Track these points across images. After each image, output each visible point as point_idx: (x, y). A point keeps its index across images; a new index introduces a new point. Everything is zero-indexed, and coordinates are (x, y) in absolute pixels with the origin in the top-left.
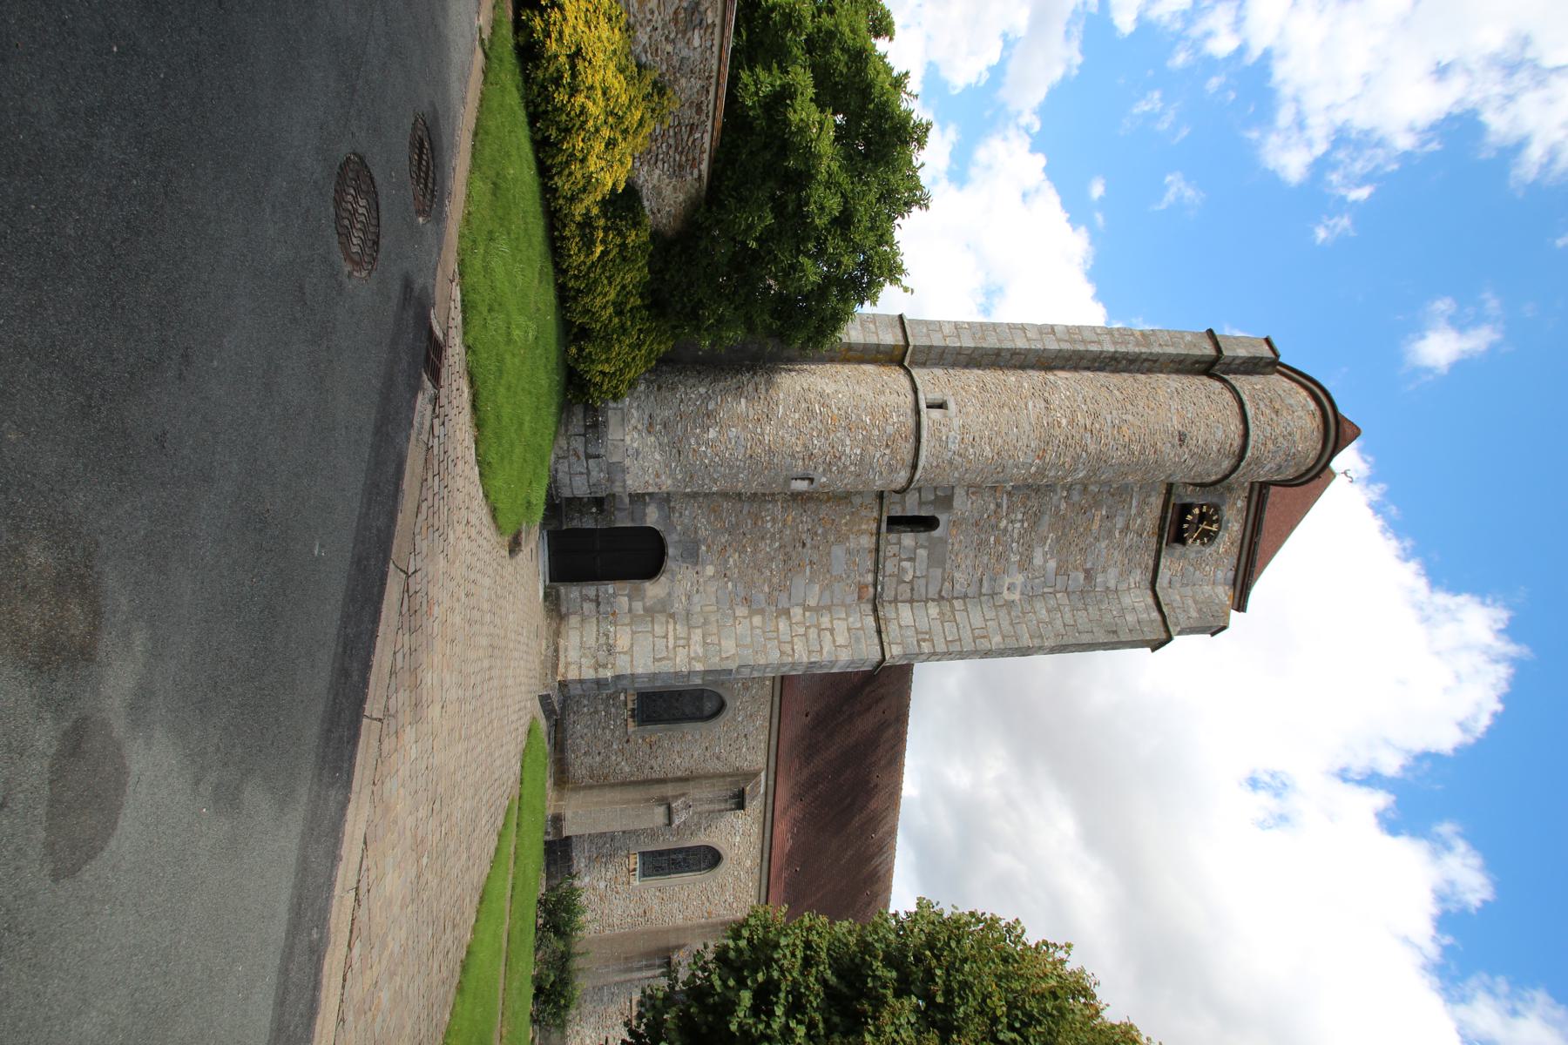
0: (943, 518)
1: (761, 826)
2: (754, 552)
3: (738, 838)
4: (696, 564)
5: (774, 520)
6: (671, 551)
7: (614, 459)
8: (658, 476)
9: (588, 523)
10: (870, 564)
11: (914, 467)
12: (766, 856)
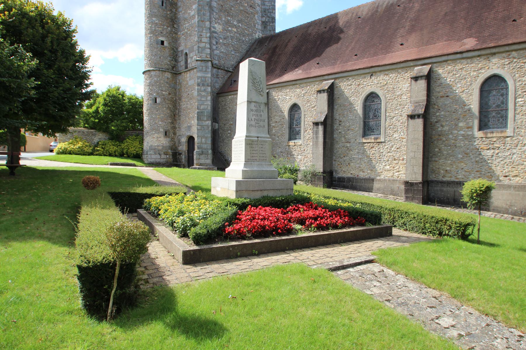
0: (185, 52)
1: (283, 88)
2: (189, 109)
3: (288, 97)
4: (191, 126)
5: (184, 105)
6: (189, 134)
7: (148, 148)
8: (154, 138)
9: (183, 157)
10: (192, 72)
11: (149, 71)
12: (294, 83)
